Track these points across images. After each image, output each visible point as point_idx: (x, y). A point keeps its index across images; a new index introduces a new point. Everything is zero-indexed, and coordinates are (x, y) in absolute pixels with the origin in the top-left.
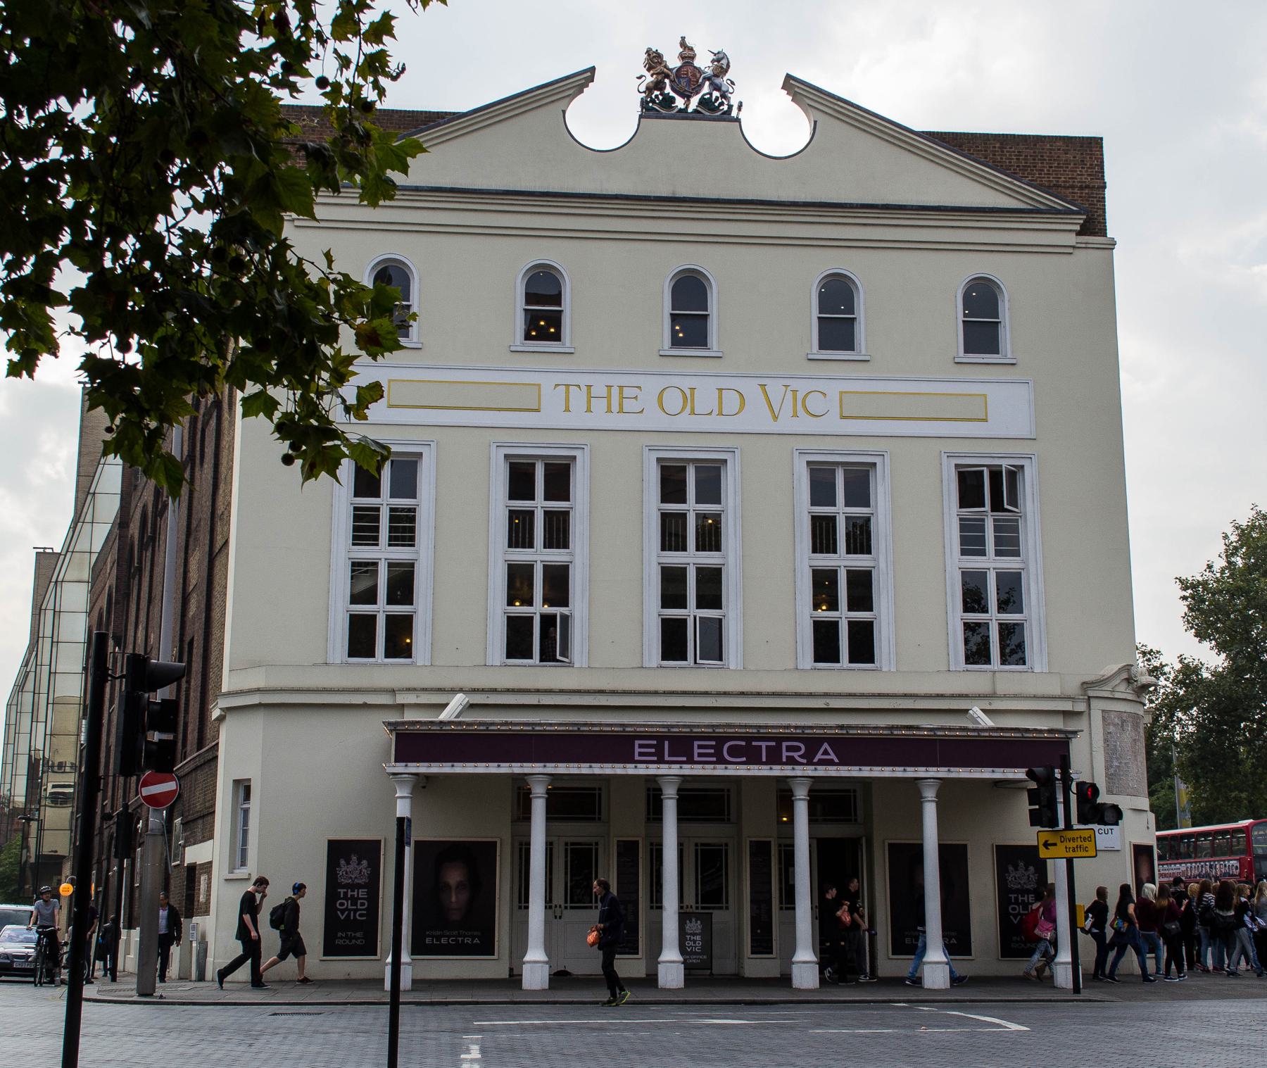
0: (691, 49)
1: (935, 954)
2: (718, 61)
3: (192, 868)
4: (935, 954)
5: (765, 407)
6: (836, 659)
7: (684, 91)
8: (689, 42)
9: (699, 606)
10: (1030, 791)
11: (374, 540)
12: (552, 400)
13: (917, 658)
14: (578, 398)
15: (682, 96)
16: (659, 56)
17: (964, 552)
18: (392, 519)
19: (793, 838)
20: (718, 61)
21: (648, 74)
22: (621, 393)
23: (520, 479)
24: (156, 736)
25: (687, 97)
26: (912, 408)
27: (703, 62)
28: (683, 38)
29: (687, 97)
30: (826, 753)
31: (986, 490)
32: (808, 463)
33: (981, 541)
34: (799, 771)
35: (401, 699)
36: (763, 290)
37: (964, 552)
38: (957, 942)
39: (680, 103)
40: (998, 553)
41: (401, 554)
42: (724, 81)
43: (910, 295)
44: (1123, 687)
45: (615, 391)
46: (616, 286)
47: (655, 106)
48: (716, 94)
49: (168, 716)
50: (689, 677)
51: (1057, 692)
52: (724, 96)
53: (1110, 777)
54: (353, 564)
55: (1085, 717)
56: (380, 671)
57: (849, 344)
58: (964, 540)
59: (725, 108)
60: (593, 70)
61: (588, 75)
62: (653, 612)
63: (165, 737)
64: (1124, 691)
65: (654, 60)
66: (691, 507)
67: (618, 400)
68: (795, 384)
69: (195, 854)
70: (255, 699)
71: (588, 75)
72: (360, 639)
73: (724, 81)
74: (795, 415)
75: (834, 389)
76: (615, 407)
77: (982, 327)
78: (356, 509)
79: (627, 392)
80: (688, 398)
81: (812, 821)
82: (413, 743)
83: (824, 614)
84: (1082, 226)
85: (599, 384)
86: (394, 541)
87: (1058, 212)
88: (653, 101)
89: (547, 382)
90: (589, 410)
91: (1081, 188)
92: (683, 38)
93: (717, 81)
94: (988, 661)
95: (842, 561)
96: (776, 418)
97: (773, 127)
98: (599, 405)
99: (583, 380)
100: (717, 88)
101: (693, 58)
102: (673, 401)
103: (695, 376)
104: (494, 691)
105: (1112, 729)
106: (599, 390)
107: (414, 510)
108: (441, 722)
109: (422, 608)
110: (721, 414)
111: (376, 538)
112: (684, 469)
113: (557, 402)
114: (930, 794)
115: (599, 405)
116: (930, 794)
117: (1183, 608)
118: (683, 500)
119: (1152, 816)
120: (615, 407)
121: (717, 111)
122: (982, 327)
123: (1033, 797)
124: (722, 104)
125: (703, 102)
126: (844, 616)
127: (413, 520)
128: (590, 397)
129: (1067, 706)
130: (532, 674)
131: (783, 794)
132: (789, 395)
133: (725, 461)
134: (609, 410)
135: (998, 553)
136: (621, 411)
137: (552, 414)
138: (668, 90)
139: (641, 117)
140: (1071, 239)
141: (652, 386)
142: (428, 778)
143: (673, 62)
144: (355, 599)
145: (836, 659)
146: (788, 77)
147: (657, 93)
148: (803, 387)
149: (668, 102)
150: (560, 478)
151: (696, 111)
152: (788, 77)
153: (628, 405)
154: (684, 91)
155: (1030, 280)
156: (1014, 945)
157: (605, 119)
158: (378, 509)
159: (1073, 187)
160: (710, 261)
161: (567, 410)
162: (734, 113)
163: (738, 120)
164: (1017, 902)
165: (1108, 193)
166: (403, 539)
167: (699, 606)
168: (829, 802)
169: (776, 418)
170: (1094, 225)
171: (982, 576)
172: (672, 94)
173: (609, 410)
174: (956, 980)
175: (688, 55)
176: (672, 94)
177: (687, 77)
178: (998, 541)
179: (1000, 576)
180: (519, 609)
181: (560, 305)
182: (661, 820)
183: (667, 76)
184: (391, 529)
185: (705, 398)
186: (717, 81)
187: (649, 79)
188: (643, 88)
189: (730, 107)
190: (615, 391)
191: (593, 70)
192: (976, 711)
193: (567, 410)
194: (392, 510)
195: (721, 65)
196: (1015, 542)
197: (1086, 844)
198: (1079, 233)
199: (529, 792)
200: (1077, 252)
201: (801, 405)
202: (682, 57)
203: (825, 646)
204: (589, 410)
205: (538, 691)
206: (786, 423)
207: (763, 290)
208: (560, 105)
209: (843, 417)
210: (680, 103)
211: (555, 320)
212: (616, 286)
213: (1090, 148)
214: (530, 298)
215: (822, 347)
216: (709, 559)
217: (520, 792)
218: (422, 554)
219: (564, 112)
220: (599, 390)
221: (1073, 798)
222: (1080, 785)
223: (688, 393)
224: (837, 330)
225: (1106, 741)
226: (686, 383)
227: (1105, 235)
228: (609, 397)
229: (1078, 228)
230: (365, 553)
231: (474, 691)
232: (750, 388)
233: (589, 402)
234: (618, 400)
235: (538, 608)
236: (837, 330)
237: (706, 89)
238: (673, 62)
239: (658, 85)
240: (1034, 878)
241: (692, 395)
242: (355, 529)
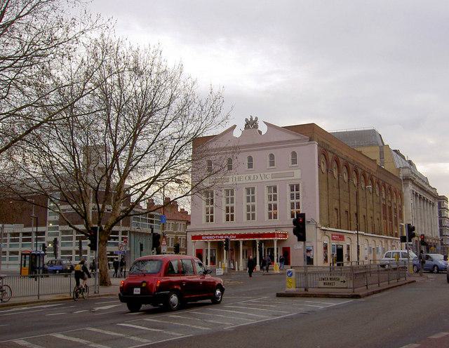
5: (261, 177)
7: (251, 124)
31: (295, 187)
36: (261, 157)
43: (283, 156)
65: (246, 120)
97: (263, 128)
102: (247, 178)
121: (256, 127)
140: (307, 143)
148: (266, 173)
154: (251, 124)
160: (251, 154)
175: (251, 119)
198: (310, 141)
201: (266, 177)
207: (261, 157)
217: (238, 242)
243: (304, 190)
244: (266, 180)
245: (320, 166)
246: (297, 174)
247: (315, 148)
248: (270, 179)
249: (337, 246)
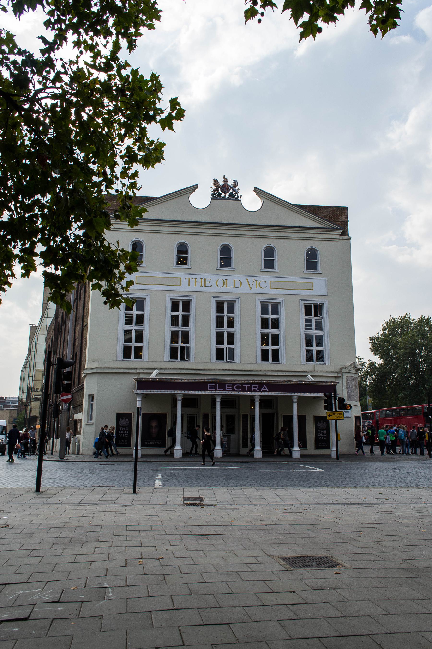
0: (227, 179)
1: (296, 448)
2: (235, 183)
3: (76, 421)
4: (296, 448)
5: (248, 285)
6: (268, 360)
7: (225, 191)
8: (226, 177)
9: (227, 344)
10: (325, 400)
11: (131, 324)
12: (185, 283)
13: (292, 360)
14: (192, 282)
15: (224, 193)
16: (217, 181)
17: (306, 329)
18: (137, 317)
19: (254, 413)
20: (235, 183)
21: (214, 186)
22: (205, 280)
23: (175, 306)
24: (65, 382)
25: (225, 193)
26: (291, 286)
27: (230, 183)
28: (224, 176)
29: (225, 193)
30: (265, 388)
31: (313, 310)
32: (261, 302)
33: (311, 326)
34: (257, 393)
35: (139, 371)
37: (306, 329)
38: (303, 444)
39: (223, 195)
40: (316, 329)
41: (139, 328)
42: (236, 189)
44: (352, 369)
45: (203, 280)
46: (204, 249)
47: (216, 196)
48: (234, 192)
49: (69, 376)
50: (225, 365)
51: (333, 370)
52: (236, 193)
53: (348, 396)
54: (125, 331)
55: (341, 378)
56: (133, 363)
57: (273, 267)
58: (306, 325)
59: (237, 196)
60: (197, 185)
61: (196, 186)
62: (214, 346)
63: (68, 382)
64: (352, 371)
65: (216, 182)
66: (226, 315)
67: (204, 283)
68: (256, 279)
69: (77, 417)
70: (95, 371)
71: (196, 187)
72: (127, 353)
73: (236, 189)
74: (257, 288)
75: (268, 280)
76: (203, 285)
77: (312, 263)
78: (126, 314)
79: (207, 280)
80: (225, 282)
81: (260, 408)
82: (142, 384)
83: (264, 347)
84: (341, 233)
85: (199, 278)
86: (137, 324)
87: (335, 229)
88: (215, 194)
89: (183, 277)
90: (195, 286)
91: (341, 222)
92: (224, 176)
93: (234, 189)
94: (313, 361)
95: (270, 331)
96: (251, 289)
97: (251, 202)
98: (199, 284)
99: (194, 277)
100: (235, 191)
101: (227, 182)
102: (221, 283)
103: (227, 276)
104: (167, 369)
105: (349, 382)
106: (198, 280)
107: (143, 315)
108: (151, 378)
109: (145, 344)
110: (234, 287)
111: (132, 323)
112: (223, 303)
113: (186, 283)
114: (295, 400)
115: (199, 284)
116: (295, 400)
117: (370, 346)
118: (223, 313)
119: (360, 408)
120: (203, 285)
121: (234, 198)
122: (312, 263)
123: (326, 402)
124: (236, 195)
125: (230, 195)
126: (270, 347)
127: (143, 318)
128: (196, 282)
129: (336, 375)
130: (178, 364)
131: (252, 400)
132: (255, 282)
133: (236, 301)
134: (201, 286)
135: (316, 329)
136: (205, 286)
137: (184, 287)
138: (220, 191)
139: (212, 199)
140: (338, 237)
142: (147, 394)
143: (221, 183)
144: (125, 341)
145: (268, 360)
146: (255, 188)
147: (216, 192)
148: (259, 279)
149: (220, 195)
150: (186, 306)
151: (228, 197)
152: (255, 188)
153: (207, 284)
154: (225, 191)
155: (325, 249)
156: (319, 445)
157: (201, 200)
158: (132, 314)
159: (339, 221)
161: (189, 285)
162: (239, 198)
163: (240, 200)
164: (320, 433)
165: (349, 224)
166: (140, 323)
167: (227, 344)
168: (266, 402)
169: (251, 289)
170: (345, 232)
171: (311, 336)
172: (221, 192)
173: (201, 286)
174: (302, 456)
175: (226, 181)
176: (221, 192)
177: (225, 187)
178: (316, 326)
179: (317, 336)
180: (174, 345)
181: (187, 254)
182: (216, 408)
183: (220, 187)
184: (136, 320)
185: (230, 283)
186: (234, 189)
187: (214, 188)
188: (212, 190)
189: (238, 196)
190: (203, 280)
191: (197, 185)
192: (309, 376)
193: (189, 285)
194: (136, 315)
195: (235, 184)
196: (321, 326)
197: (340, 416)
198: (340, 235)
199: (176, 399)
200: (340, 241)
201: (258, 285)
202: (224, 181)
203: (265, 356)
204: (195, 286)
205: (179, 369)
206: (254, 290)
208: (188, 195)
209: (271, 289)
210: (223, 195)
211: (186, 259)
212: (204, 249)
213: (344, 210)
214: (178, 252)
215: (265, 268)
216: (231, 330)
217: (174, 398)
218: (146, 328)
219: (189, 197)
220: (198, 280)
221: (337, 402)
222: (339, 398)
223: (225, 281)
224: (269, 263)
225: (347, 385)
226: (224, 278)
227: (348, 236)
228: (201, 282)
229: (340, 233)
230: (128, 327)
231: (161, 369)
232: (243, 279)
233: (195, 283)
234: (204, 283)
235: (180, 344)
236: (269, 263)
237: (231, 191)
238: (221, 183)
239: (217, 190)
240: (325, 425)
241: (226, 281)
242: (126, 320)
244: (259, 290)
248: (268, 290)
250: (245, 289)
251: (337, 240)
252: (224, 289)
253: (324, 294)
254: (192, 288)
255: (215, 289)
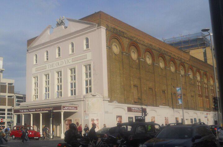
12: (47, 66)
75: (71, 58)
85: (51, 64)
102: (57, 64)
115: (51, 66)
137: (47, 69)
141: (55, 62)
148: (68, 59)
206: (67, 64)
220: (51, 65)
232: (63, 60)
243: (94, 70)
244: (69, 64)
245: (109, 48)
246: (89, 56)
247: (103, 31)
248: (71, 63)
249: (136, 117)
250: (64, 65)
251: (95, 30)
252: (58, 67)
253: (91, 59)
254: (50, 69)
255: (56, 67)
